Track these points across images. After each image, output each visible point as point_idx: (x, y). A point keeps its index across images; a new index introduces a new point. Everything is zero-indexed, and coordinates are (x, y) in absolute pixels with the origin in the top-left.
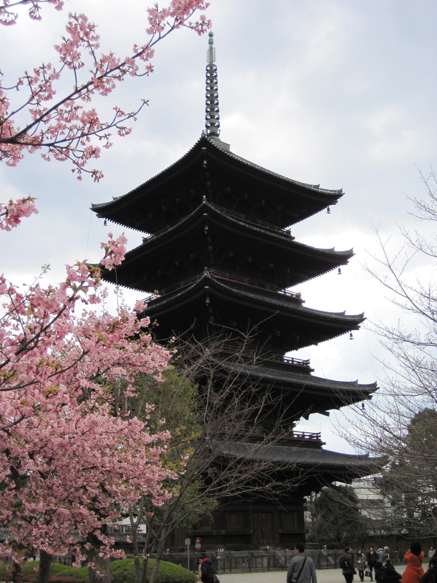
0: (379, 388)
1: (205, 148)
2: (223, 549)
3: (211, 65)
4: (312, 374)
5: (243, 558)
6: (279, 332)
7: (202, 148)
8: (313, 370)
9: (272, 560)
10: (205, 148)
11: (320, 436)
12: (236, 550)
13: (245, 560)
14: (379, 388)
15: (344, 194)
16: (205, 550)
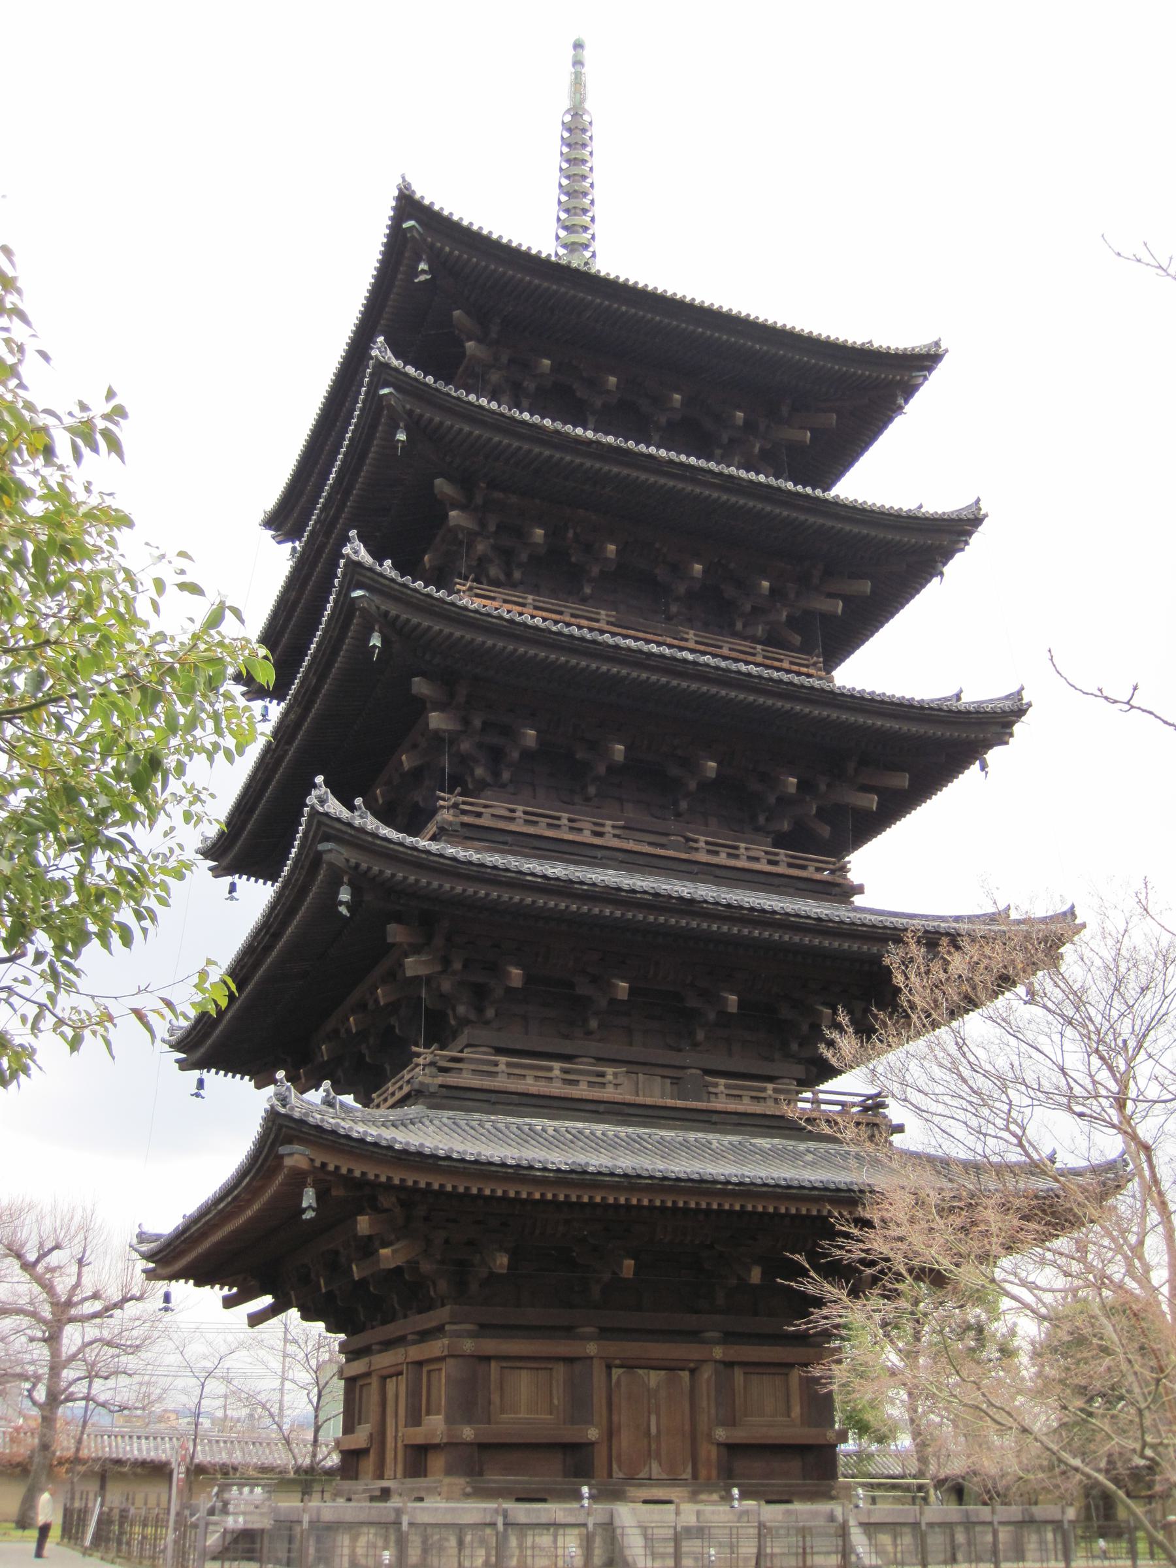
0: (1084, 926)
1: (411, 223)
2: (258, 1490)
3: (576, 112)
4: (858, 900)
5: (460, 1529)
6: (713, 764)
7: (404, 226)
8: (859, 889)
9: (598, 1541)
10: (411, 223)
11: (883, 1105)
12: (519, 1500)
13: (468, 1538)
14: (1084, 926)
15: (946, 351)
16: (422, 1494)
